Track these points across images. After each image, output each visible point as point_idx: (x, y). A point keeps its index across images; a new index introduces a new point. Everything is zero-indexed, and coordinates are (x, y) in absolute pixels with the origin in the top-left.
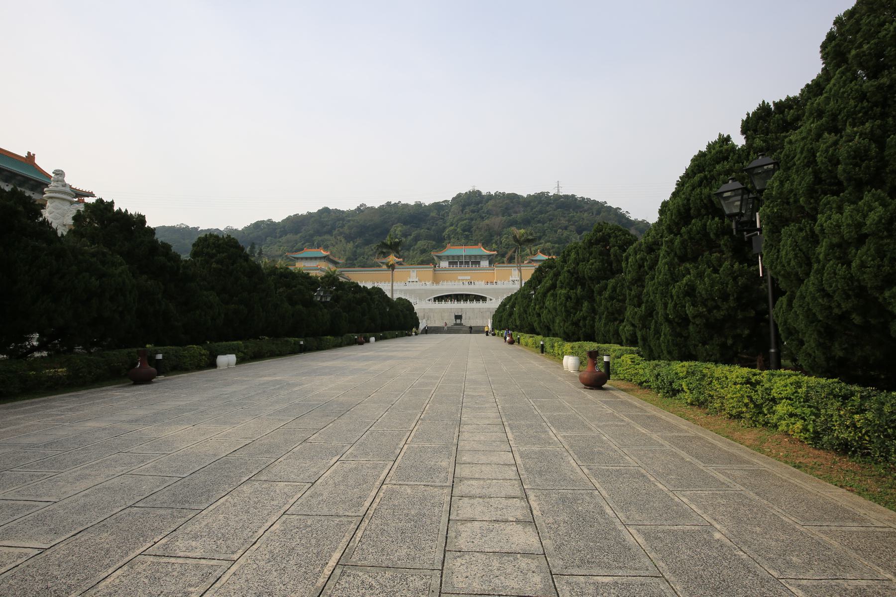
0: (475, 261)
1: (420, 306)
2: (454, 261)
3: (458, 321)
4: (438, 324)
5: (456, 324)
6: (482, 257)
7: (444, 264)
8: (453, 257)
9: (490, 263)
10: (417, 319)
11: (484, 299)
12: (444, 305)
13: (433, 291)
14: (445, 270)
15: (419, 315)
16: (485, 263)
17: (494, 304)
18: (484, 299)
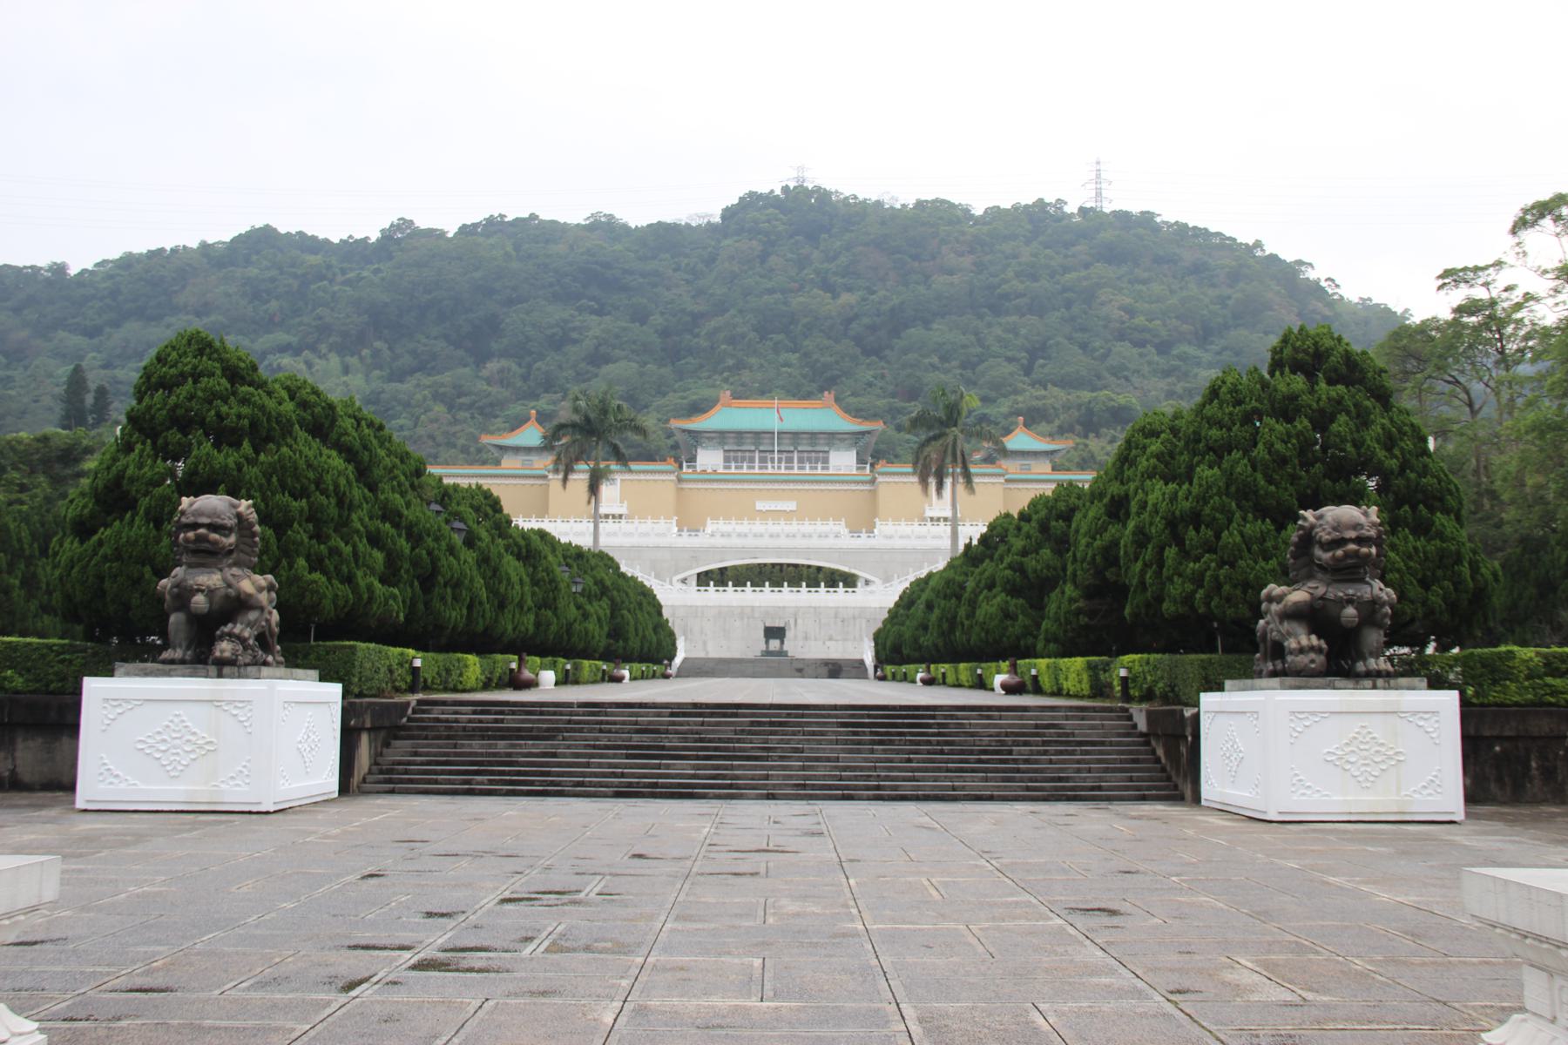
0: (813, 444)
1: (676, 597)
2: (739, 443)
3: (774, 644)
4: (715, 651)
5: (768, 653)
6: (833, 438)
7: (709, 458)
8: (739, 435)
9: (861, 461)
10: (672, 636)
11: (849, 581)
12: (731, 596)
13: (695, 554)
14: (711, 478)
15: (676, 625)
16: (843, 461)
17: (879, 597)
18: (849, 581)
